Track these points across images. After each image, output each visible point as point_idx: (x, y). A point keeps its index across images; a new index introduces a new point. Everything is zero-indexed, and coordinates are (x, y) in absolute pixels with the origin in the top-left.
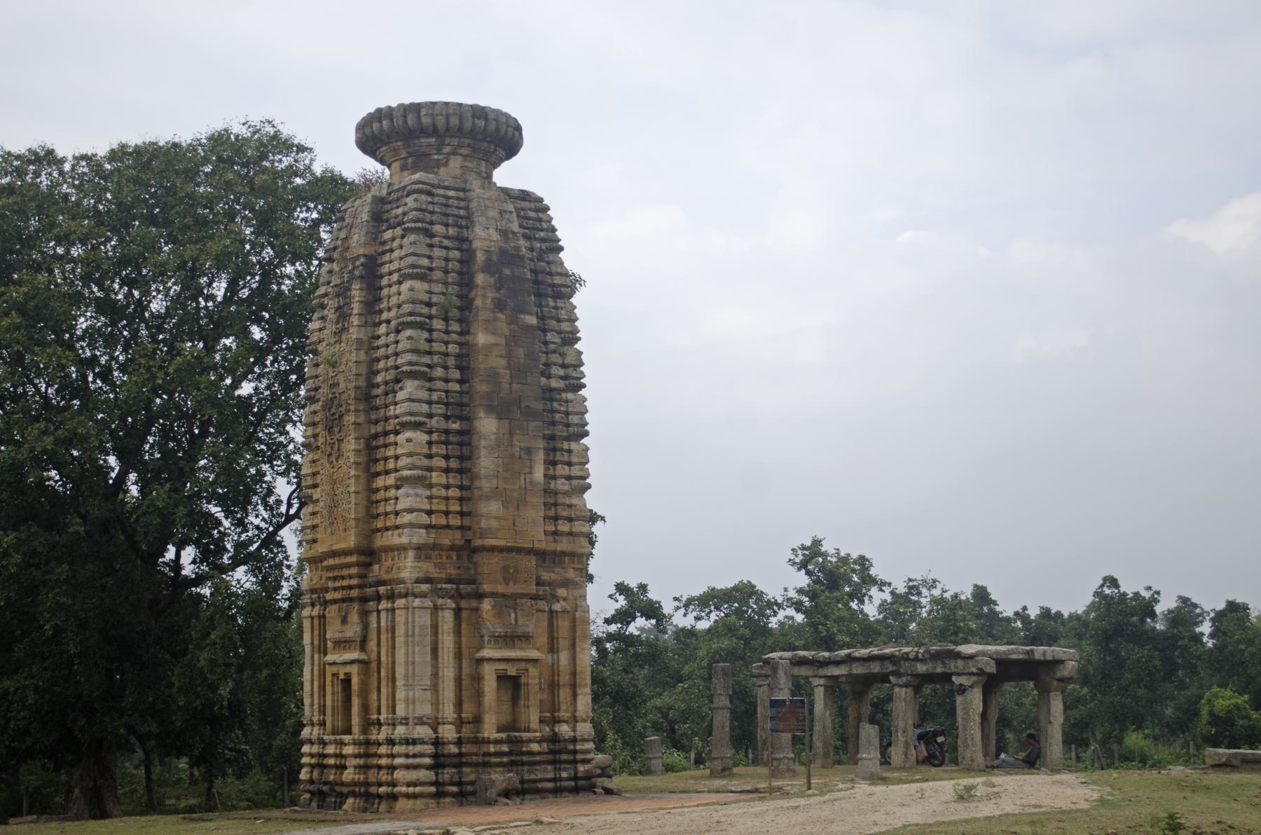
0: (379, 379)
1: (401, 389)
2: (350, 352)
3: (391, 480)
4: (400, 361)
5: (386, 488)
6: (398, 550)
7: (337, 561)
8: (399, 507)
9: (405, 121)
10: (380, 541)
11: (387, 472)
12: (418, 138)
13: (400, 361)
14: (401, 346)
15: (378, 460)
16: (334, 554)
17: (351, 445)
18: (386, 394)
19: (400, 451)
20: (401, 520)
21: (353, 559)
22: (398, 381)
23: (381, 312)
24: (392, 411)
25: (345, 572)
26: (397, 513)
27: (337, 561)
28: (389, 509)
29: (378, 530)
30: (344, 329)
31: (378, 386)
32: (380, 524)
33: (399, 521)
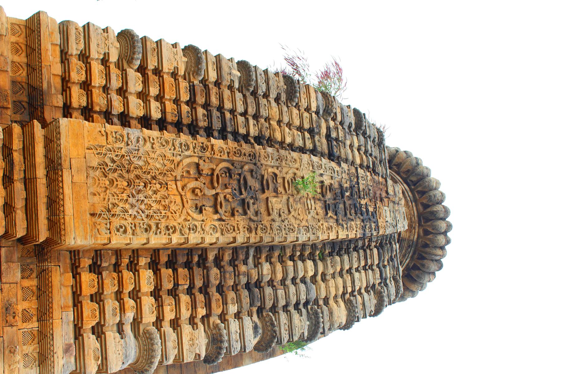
0: (266, 268)
1: (255, 328)
2: (307, 229)
3: (149, 318)
4: (283, 317)
5: (135, 295)
6: (40, 332)
7: (41, 172)
8: (111, 336)
9: (432, 260)
10: (61, 282)
11: (156, 294)
12: (412, 257)
13: (283, 317)
14: (296, 316)
15: (175, 270)
16: (54, 166)
17: (208, 233)
18: (248, 286)
19: (186, 329)
20: (91, 341)
21: (43, 235)
22: (260, 311)
23: (322, 259)
24: (233, 309)
25: (19, 186)
26: (98, 331)
27: (41, 172)
28: (111, 304)
29: (76, 275)
30: (326, 208)
31: (257, 265)
32: (88, 279)
33: (91, 341)
